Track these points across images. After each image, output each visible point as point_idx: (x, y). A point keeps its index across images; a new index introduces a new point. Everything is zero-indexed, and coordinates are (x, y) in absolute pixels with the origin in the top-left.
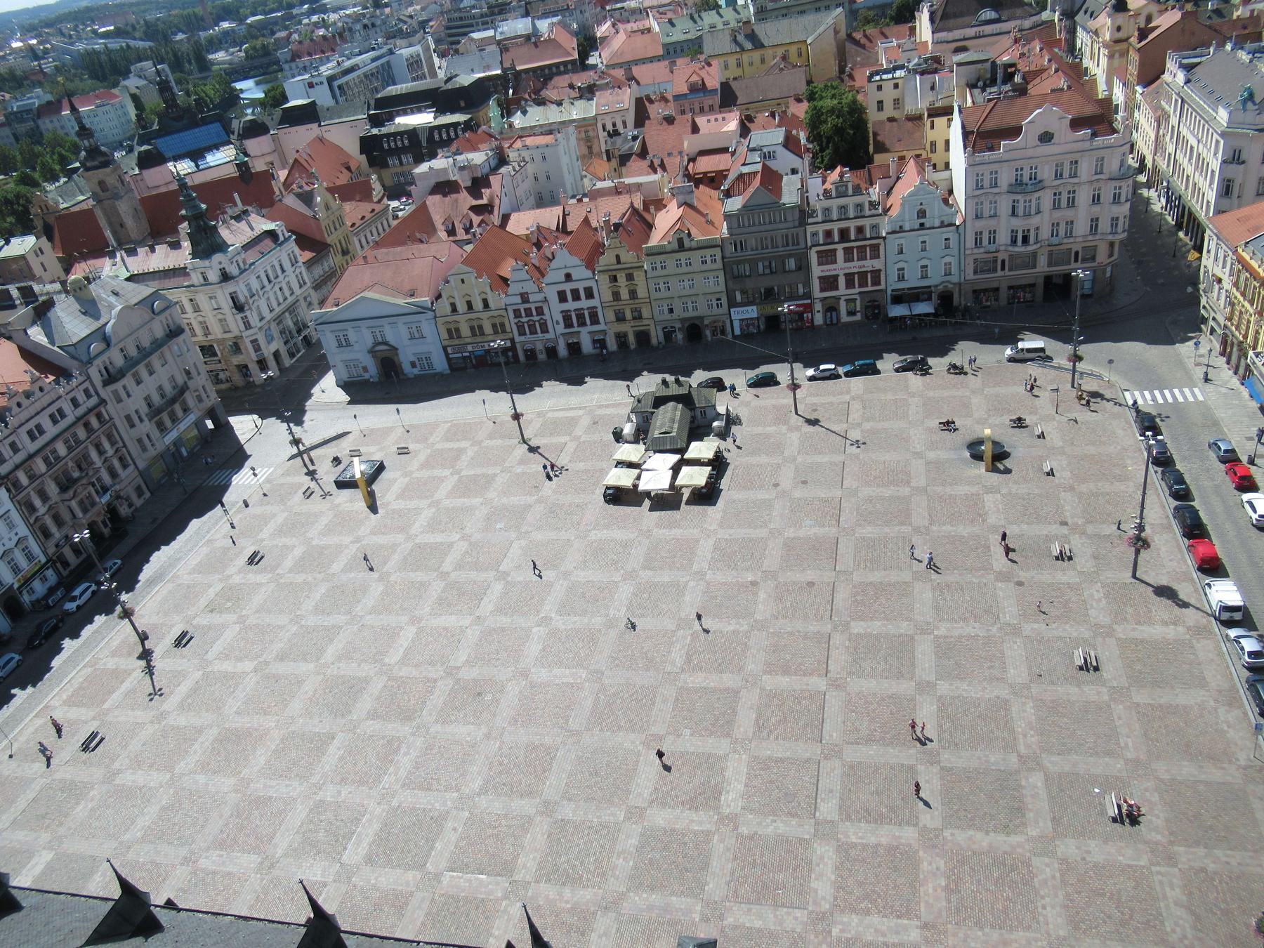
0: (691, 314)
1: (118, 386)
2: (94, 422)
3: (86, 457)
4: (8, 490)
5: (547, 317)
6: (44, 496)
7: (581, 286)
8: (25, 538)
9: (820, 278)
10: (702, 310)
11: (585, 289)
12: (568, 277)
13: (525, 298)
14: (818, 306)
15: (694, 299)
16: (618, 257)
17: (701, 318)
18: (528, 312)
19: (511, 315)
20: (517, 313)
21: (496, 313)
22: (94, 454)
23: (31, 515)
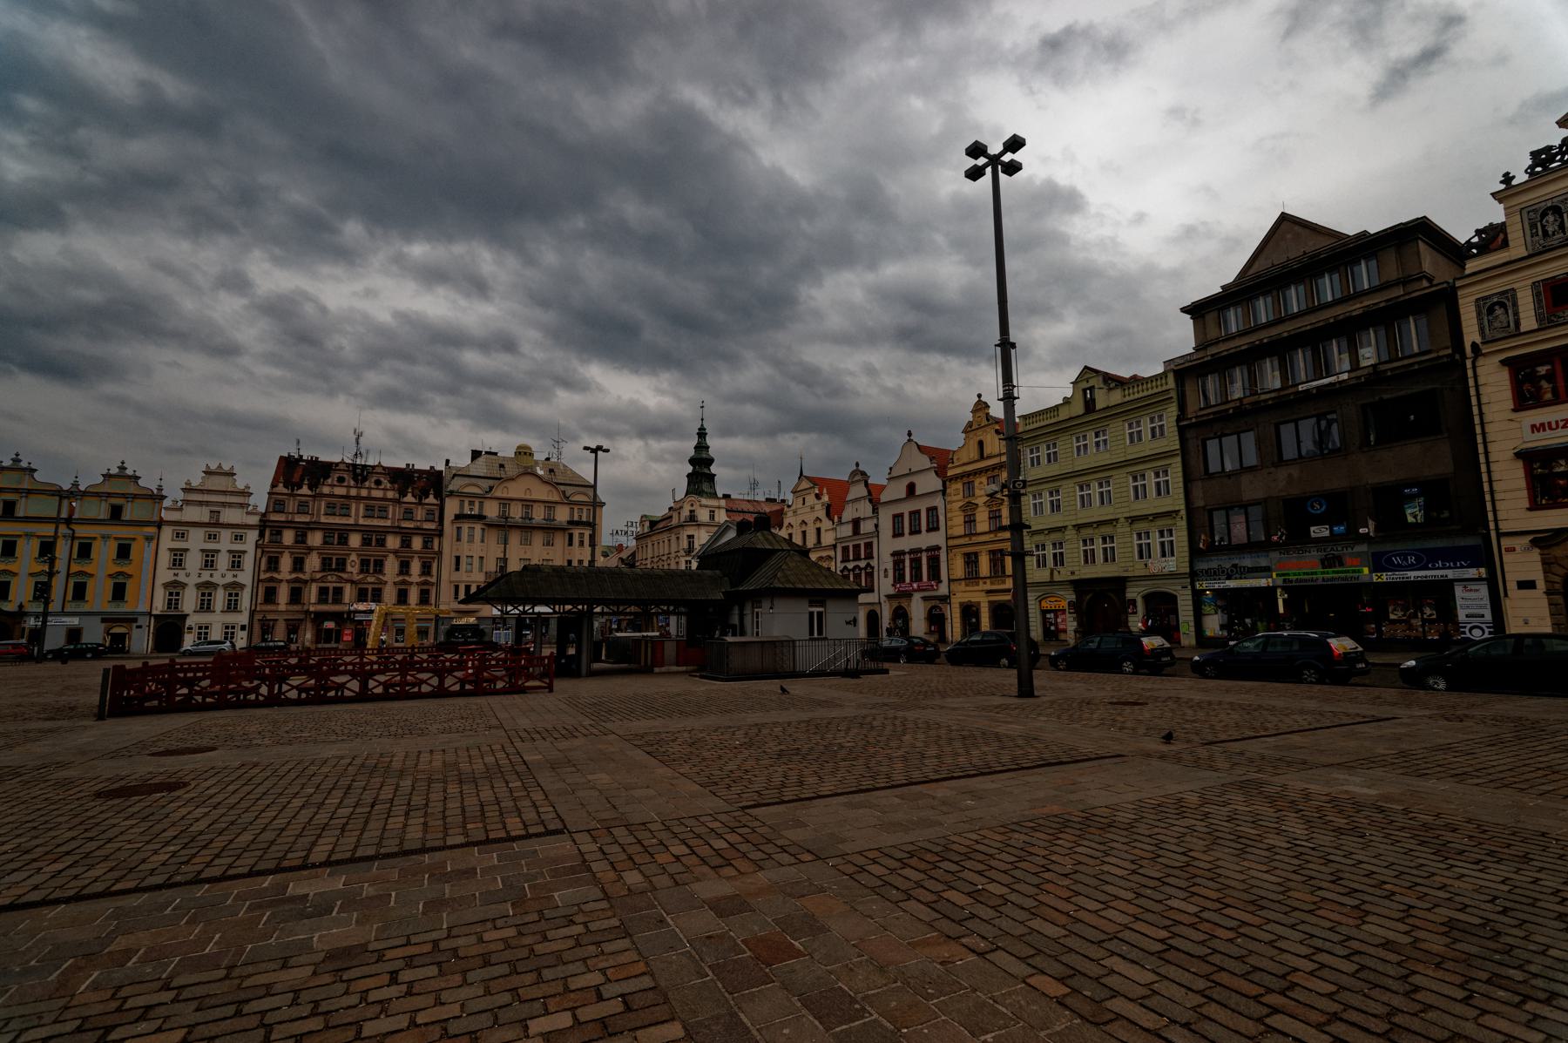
0: (1100, 570)
1: (465, 527)
2: (417, 543)
3: (379, 565)
4: (262, 535)
5: (874, 563)
6: (298, 564)
7: (922, 506)
8: (242, 586)
9: (1527, 457)
10: (1125, 563)
11: (928, 510)
12: (911, 489)
13: (856, 523)
14: (1522, 563)
15: (1106, 530)
16: (981, 443)
17: (1120, 583)
18: (857, 547)
19: (839, 558)
20: (845, 549)
21: (824, 554)
22: (391, 566)
23: (268, 569)
